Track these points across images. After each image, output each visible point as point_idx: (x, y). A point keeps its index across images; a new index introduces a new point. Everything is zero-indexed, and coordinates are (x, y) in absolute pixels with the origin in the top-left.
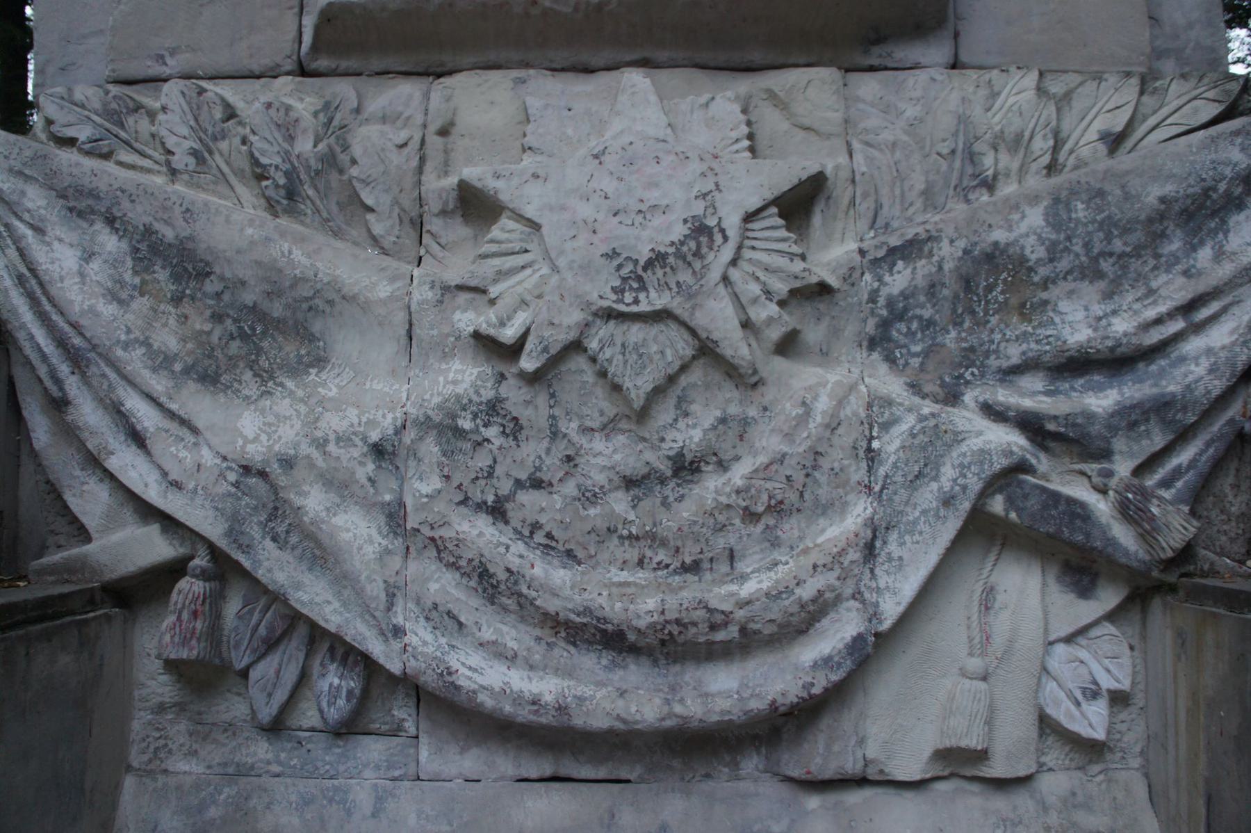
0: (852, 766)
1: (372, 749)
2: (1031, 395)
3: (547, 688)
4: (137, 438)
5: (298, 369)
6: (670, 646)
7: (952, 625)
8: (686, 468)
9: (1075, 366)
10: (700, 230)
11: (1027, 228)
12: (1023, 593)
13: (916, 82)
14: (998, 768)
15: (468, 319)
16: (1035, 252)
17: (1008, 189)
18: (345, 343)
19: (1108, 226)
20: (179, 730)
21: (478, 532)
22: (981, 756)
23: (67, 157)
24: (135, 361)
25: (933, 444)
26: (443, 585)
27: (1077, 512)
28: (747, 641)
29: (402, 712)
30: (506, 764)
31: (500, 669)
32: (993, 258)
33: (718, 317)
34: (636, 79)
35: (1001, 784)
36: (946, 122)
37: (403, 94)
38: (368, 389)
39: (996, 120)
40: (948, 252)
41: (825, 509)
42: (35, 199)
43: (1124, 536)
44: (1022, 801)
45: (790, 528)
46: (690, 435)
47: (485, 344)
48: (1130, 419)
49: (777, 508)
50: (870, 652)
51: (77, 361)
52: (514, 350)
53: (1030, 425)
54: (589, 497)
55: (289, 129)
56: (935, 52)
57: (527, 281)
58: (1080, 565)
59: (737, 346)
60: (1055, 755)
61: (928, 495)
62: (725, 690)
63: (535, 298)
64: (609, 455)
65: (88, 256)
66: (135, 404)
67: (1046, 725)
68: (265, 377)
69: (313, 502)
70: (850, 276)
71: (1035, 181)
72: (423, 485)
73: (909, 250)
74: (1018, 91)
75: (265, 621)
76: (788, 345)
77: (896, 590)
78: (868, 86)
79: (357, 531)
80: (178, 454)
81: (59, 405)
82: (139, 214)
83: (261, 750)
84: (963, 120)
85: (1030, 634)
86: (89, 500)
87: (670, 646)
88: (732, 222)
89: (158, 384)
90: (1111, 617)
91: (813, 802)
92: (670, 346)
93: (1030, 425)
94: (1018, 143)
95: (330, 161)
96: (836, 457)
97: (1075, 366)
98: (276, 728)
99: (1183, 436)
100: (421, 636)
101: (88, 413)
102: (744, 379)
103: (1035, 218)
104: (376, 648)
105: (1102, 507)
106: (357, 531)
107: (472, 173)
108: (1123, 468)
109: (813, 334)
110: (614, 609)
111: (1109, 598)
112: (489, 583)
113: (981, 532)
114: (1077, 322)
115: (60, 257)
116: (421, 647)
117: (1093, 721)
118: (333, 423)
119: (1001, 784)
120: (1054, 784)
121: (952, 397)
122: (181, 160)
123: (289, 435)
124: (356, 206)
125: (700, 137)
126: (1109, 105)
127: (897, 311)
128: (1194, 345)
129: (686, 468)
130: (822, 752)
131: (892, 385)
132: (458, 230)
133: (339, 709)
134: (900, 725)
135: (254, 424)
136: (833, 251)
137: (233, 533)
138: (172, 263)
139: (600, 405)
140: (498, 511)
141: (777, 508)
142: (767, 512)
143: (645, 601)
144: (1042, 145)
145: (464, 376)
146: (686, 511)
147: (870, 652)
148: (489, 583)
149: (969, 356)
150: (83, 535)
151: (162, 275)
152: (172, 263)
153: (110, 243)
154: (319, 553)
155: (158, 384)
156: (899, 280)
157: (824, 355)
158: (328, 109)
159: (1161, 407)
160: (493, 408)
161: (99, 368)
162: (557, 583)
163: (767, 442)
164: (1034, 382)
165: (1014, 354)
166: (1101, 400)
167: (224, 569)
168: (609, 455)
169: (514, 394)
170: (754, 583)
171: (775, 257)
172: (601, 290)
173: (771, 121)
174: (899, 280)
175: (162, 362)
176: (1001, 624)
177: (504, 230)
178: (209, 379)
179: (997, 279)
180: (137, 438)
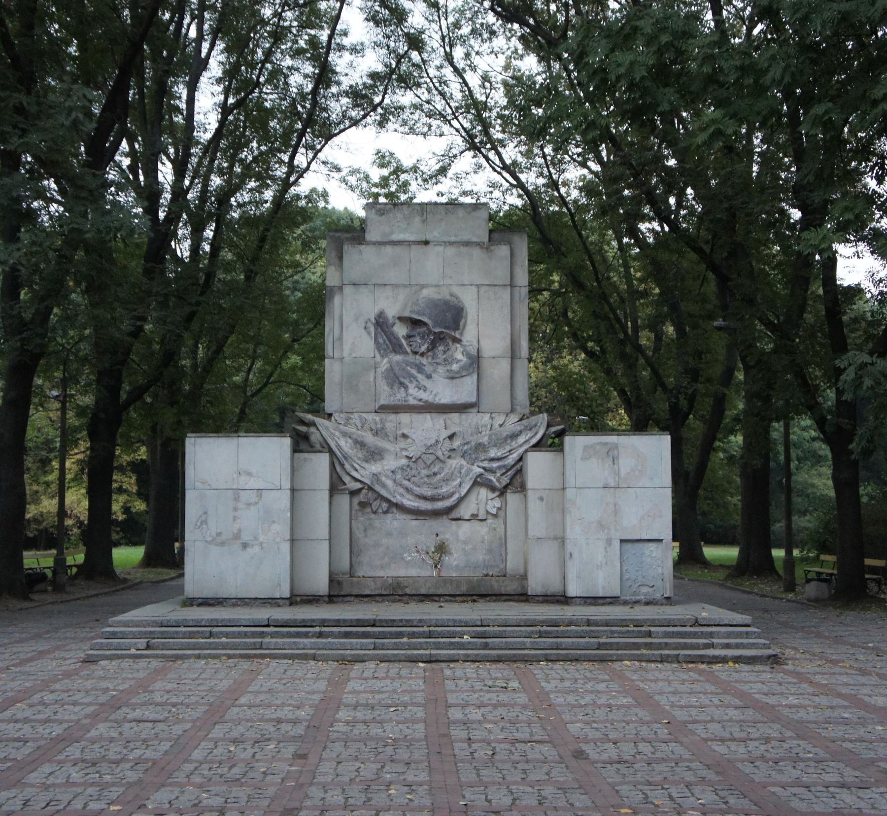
0: (458, 516)
1: (390, 515)
2: (486, 464)
3: (416, 504)
4: (356, 470)
5: (380, 460)
6: (433, 499)
7: (473, 497)
8: (435, 474)
9: (492, 460)
10: (437, 441)
11: (485, 440)
12: (484, 492)
13: (471, 415)
14: (480, 518)
15: (405, 453)
16: (486, 443)
17: (483, 433)
18: (387, 456)
19: (498, 439)
20: (360, 514)
21: (406, 483)
22: (477, 515)
23: (341, 426)
24: (355, 459)
25: (469, 471)
26: (401, 490)
27: (491, 481)
28: (444, 498)
29: (394, 510)
30: (409, 517)
31: (409, 502)
32: (480, 444)
33: (439, 454)
34: (428, 416)
35: (481, 520)
36: (474, 423)
37: (392, 417)
38: (390, 463)
39: (483, 422)
40: (473, 443)
41: (454, 480)
42: (337, 433)
43: (497, 484)
44: (484, 523)
45: (449, 483)
46: (436, 470)
47: (407, 457)
48: (499, 468)
49: (448, 480)
50: (461, 500)
51: (346, 458)
52: (411, 458)
53: (484, 468)
54: (422, 478)
55: (376, 423)
56: (475, 410)
57: (412, 448)
58: (493, 489)
59: (442, 457)
60: (490, 517)
61: (468, 478)
62: (440, 505)
63: (413, 452)
64: (424, 472)
65: (346, 442)
66: (355, 465)
67: (488, 512)
68: (375, 461)
69: (384, 479)
70: (459, 447)
71: (488, 432)
72: (399, 476)
73: (467, 443)
74: (487, 417)
75: (375, 496)
76: (449, 457)
77: (464, 491)
78: (464, 416)
79: (389, 483)
80: (362, 471)
81: (342, 465)
82: (354, 437)
83: (373, 516)
84: (477, 423)
85: (484, 500)
86: (346, 479)
87: (433, 499)
88: (441, 440)
89: (359, 462)
90: (498, 496)
91: (454, 522)
92: (433, 458)
93: (484, 468)
94: (486, 426)
95: (383, 428)
96: (456, 473)
97: (492, 460)
98: (375, 513)
99: (510, 470)
100: (398, 497)
101: (347, 466)
102: (443, 462)
103: (487, 438)
104: (392, 499)
105: (494, 480)
106: (389, 483)
107: (405, 431)
108: (498, 475)
109: (453, 455)
110: (425, 494)
111: (497, 493)
112: (408, 490)
113: (475, 483)
114: (493, 453)
115: (342, 443)
116: (398, 499)
117: (494, 511)
118: (386, 468)
119: (481, 520)
120: (489, 521)
121: (473, 464)
122: (359, 427)
123: (380, 469)
124: (387, 435)
125: (438, 427)
126: (499, 420)
127: (465, 452)
128: (511, 457)
129: (435, 474)
130: (454, 515)
131: (464, 462)
132: (402, 439)
133: (385, 509)
134: (465, 511)
135: (374, 468)
136: (457, 443)
137: (372, 483)
138: (360, 444)
139: (423, 465)
140: (409, 480)
141: (448, 480)
142: (446, 480)
143: (429, 493)
144: (489, 426)
145: (404, 461)
146: (435, 480)
147: (461, 500)
148: (408, 490)
149: (476, 458)
150: (345, 484)
151: (358, 446)
152: (360, 444)
153: (350, 440)
154: (384, 486)
155: (359, 462)
156: (466, 447)
157: (455, 458)
158: (381, 420)
159: (504, 466)
160: (408, 466)
161: (350, 460)
162: (417, 490)
163: (446, 471)
164: (486, 462)
165: (483, 458)
166: (495, 465)
167: (370, 488)
168: (424, 472)
169: (411, 464)
170: (444, 490)
171: (447, 445)
172: (423, 450)
173: (449, 422)
174: (466, 447)
175: (359, 459)
176: (480, 497)
177: (409, 440)
178: (367, 461)
179: (480, 447)
180: (356, 470)
